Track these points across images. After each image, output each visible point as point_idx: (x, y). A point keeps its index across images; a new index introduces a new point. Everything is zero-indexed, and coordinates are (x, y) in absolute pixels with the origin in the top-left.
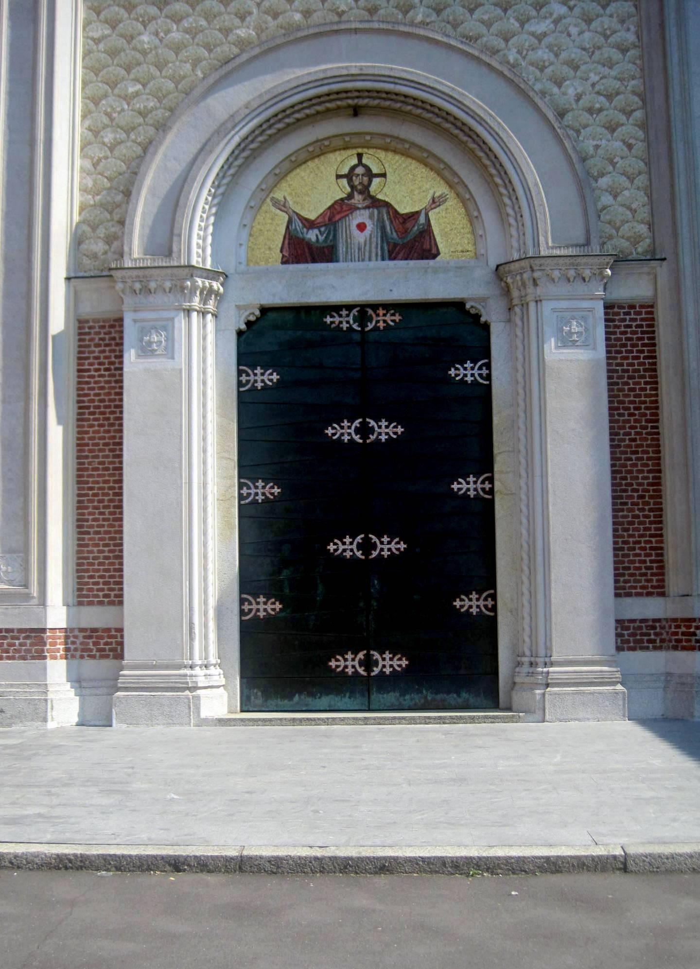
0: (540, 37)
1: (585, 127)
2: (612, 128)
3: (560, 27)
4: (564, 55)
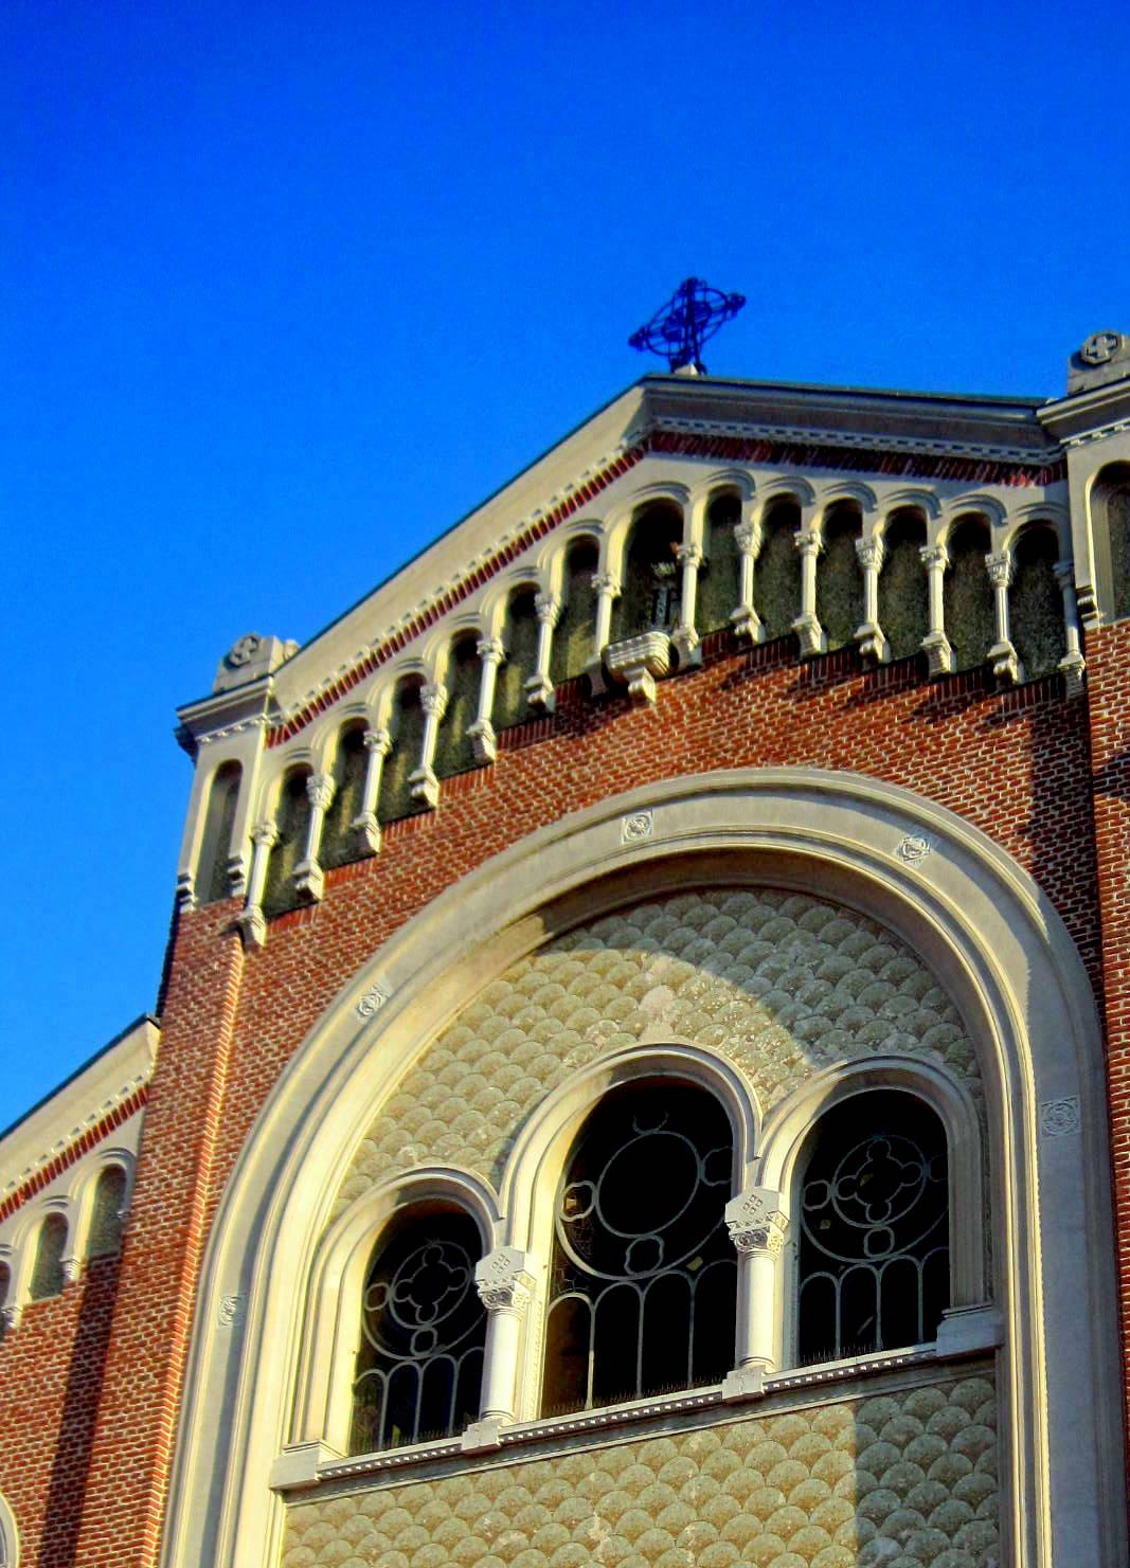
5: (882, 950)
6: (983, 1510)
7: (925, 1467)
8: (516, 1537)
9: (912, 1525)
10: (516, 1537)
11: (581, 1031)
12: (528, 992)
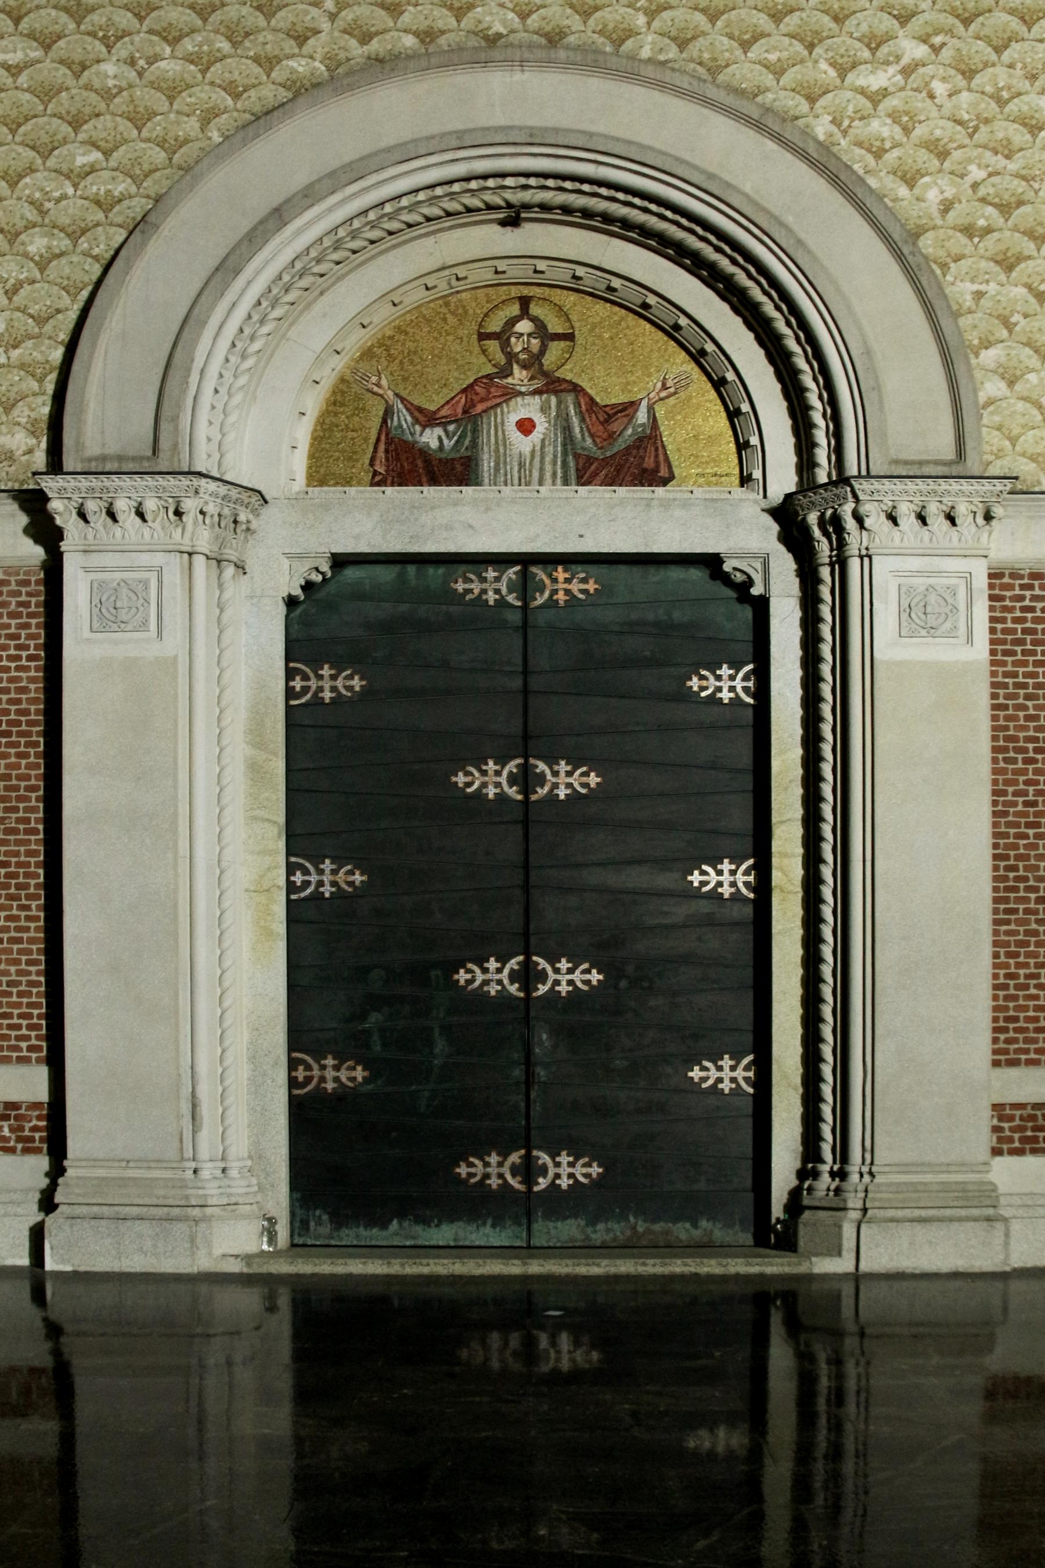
0: (876, 98)
1: (957, 259)
3: (915, 80)
4: (919, 131)
9: (950, 32)
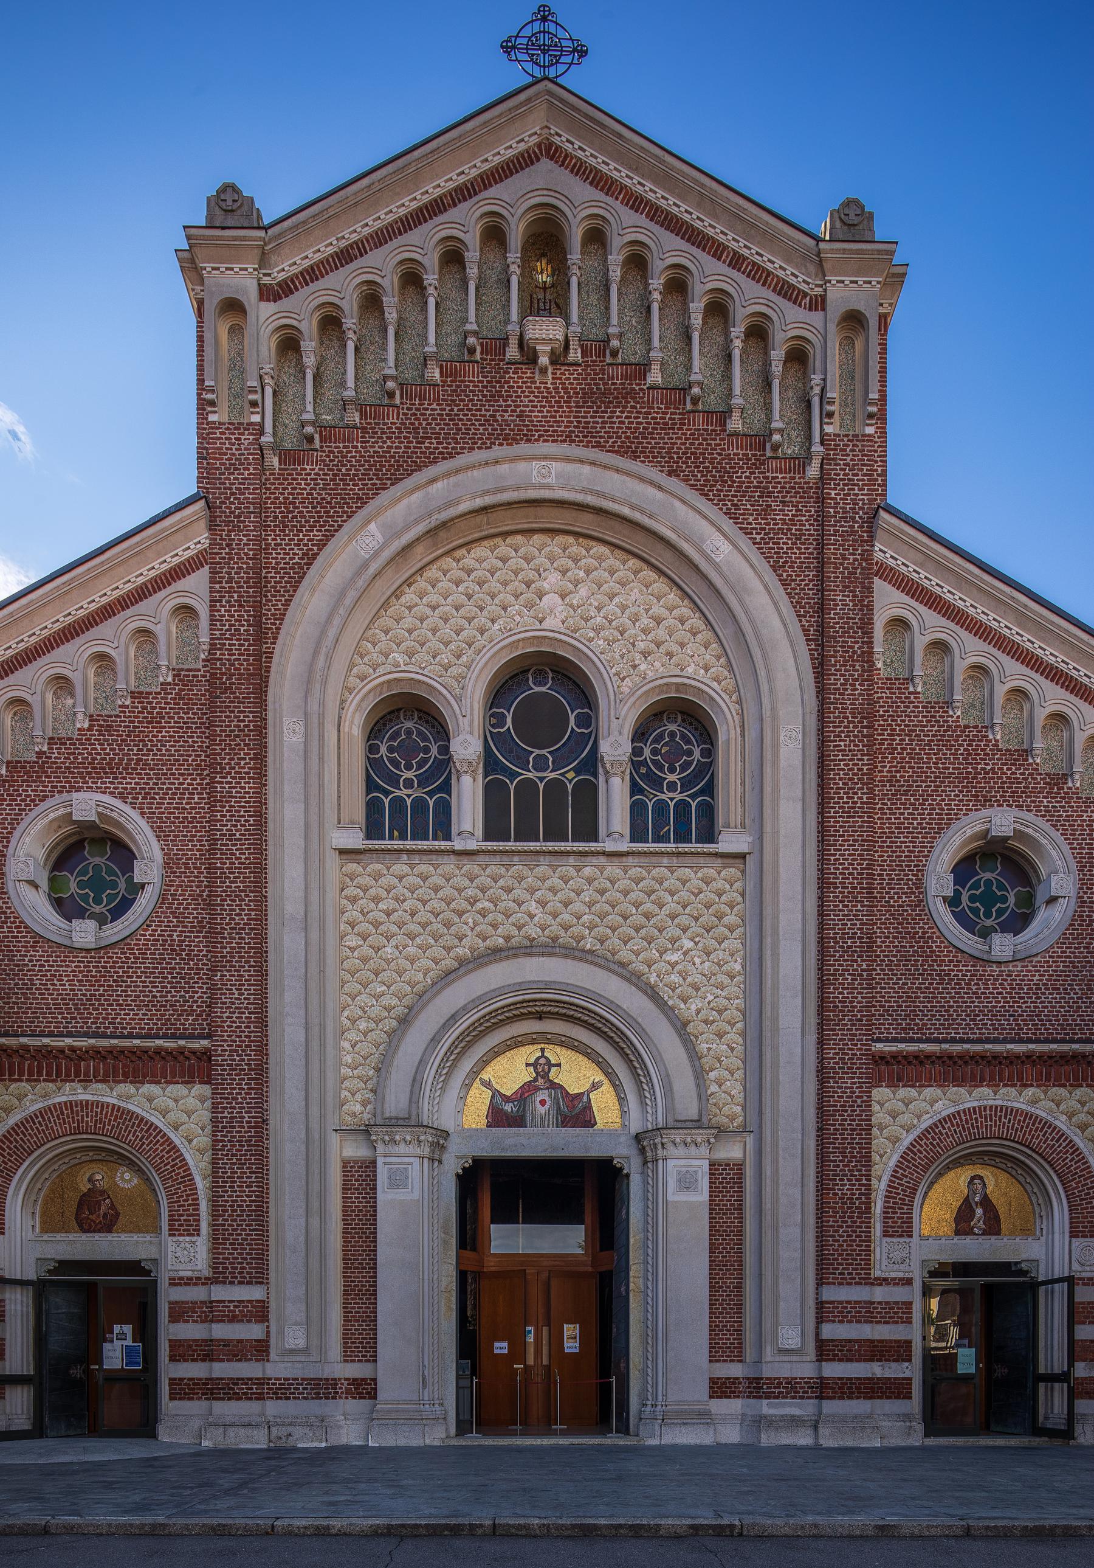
0: (673, 965)
2: (720, 1035)
5: (685, 610)
6: (736, 934)
7: (708, 908)
8: (487, 904)
10: (487, 904)
11: (505, 609)
12: (469, 572)
